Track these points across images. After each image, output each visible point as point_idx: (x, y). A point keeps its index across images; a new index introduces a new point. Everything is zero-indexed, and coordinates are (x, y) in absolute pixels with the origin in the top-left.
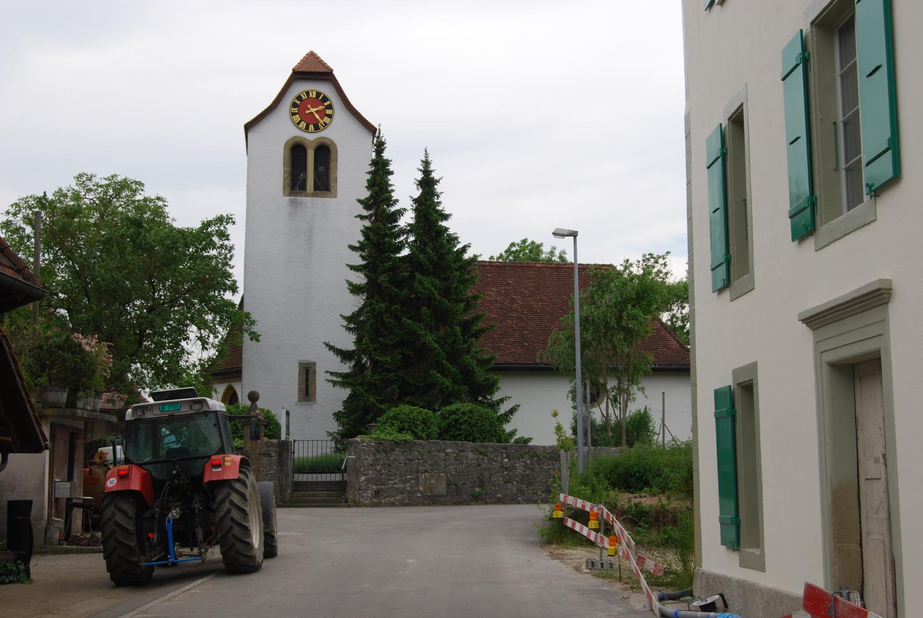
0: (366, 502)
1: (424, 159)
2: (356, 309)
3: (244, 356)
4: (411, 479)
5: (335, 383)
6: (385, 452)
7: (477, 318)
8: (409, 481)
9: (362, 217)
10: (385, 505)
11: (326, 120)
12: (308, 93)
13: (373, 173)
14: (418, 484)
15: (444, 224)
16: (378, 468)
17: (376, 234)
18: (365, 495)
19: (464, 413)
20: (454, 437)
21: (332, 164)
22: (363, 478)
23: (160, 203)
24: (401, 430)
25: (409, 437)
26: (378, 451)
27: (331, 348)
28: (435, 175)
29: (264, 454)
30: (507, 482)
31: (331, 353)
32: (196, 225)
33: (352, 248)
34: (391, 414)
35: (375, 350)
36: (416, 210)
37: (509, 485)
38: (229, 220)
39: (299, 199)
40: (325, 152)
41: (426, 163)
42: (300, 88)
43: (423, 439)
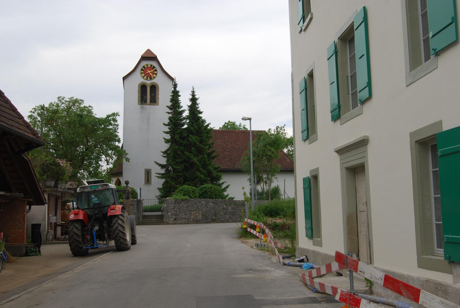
3: (123, 167)
5: (159, 177)
6: (178, 203)
7: (213, 152)
8: (187, 214)
9: (169, 113)
10: (178, 224)
11: (154, 75)
12: (147, 65)
13: (173, 96)
14: (191, 215)
15: (200, 115)
17: (174, 119)
19: (208, 188)
20: (205, 197)
21: (157, 92)
22: (170, 214)
23: (90, 108)
24: (184, 195)
25: (187, 197)
27: (157, 163)
28: (197, 97)
29: (131, 205)
30: (225, 214)
31: (157, 165)
32: (104, 116)
34: (181, 189)
35: (174, 164)
36: (189, 110)
37: (226, 216)
38: (117, 114)
39: (144, 106)
40: (154, 88)
41: (193, 92)
42: (144, 63)
43: (191, 198)
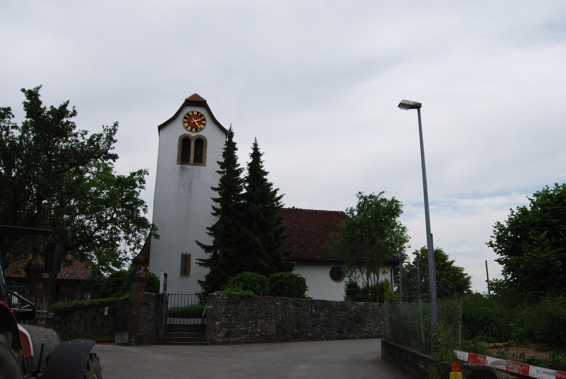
0: (220, 341)
2: (215, 223)
3: (151, 250)
4: (252, 323)
5: (200, 265)
7: (283, 229)
8: (250, 325)
9: (219, 172)
11: (202, 126)
12: (192, 112)
15: (265, 177)
16: (229, 315)
18: (219, 335)
19: (286, 278)
20: (279, 295)
21: (204, 149)
24: (245, 289)
25: (252, 293)
26: (229, 303)
27: (199, 244)
28: (261, 151)
30: (314, 325)
31: (199, 247)
32: (127, 175)
33: (213, 189)
34: (238, 277)
36: (249, 169)
37: (316, 328)
38: (146, 172)
39: (186, 166)
40: (201, 143)
41: (256, 145)
42: (189, 110)
43: (260, 295)
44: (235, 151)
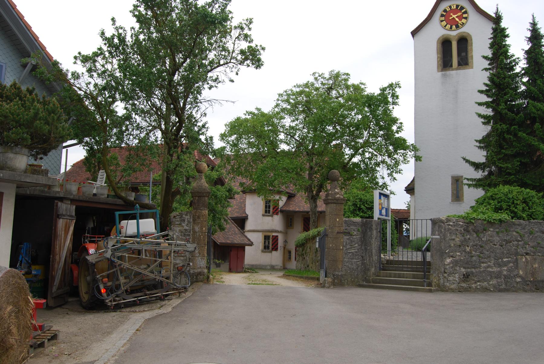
0: (453, 286)
1: (531, 22)
2: (485, 133)
4: (509, 262)
6: (477, 232)
8: (506, 264)
9: (486, 69)
10: (476, 290)
11: (464, 21)
12: (450, 7)
13: (494, 37)
14: (517, 267)
16: (468, 249)
17: (498, 78)
18: (451, 278)
21: (469, 48)
22: (448, 260)
23: (363, 87)
24: (497, 210)
26: (467, 231)
29: (344, 233)
31: (467, 164)
33: (481, 92)
35: (499, 159)
38: (398, 85)
39: (448, 72)
40: (464, 42)
41: (534, 24)
43: (520, 218)
44: (507, 39)
